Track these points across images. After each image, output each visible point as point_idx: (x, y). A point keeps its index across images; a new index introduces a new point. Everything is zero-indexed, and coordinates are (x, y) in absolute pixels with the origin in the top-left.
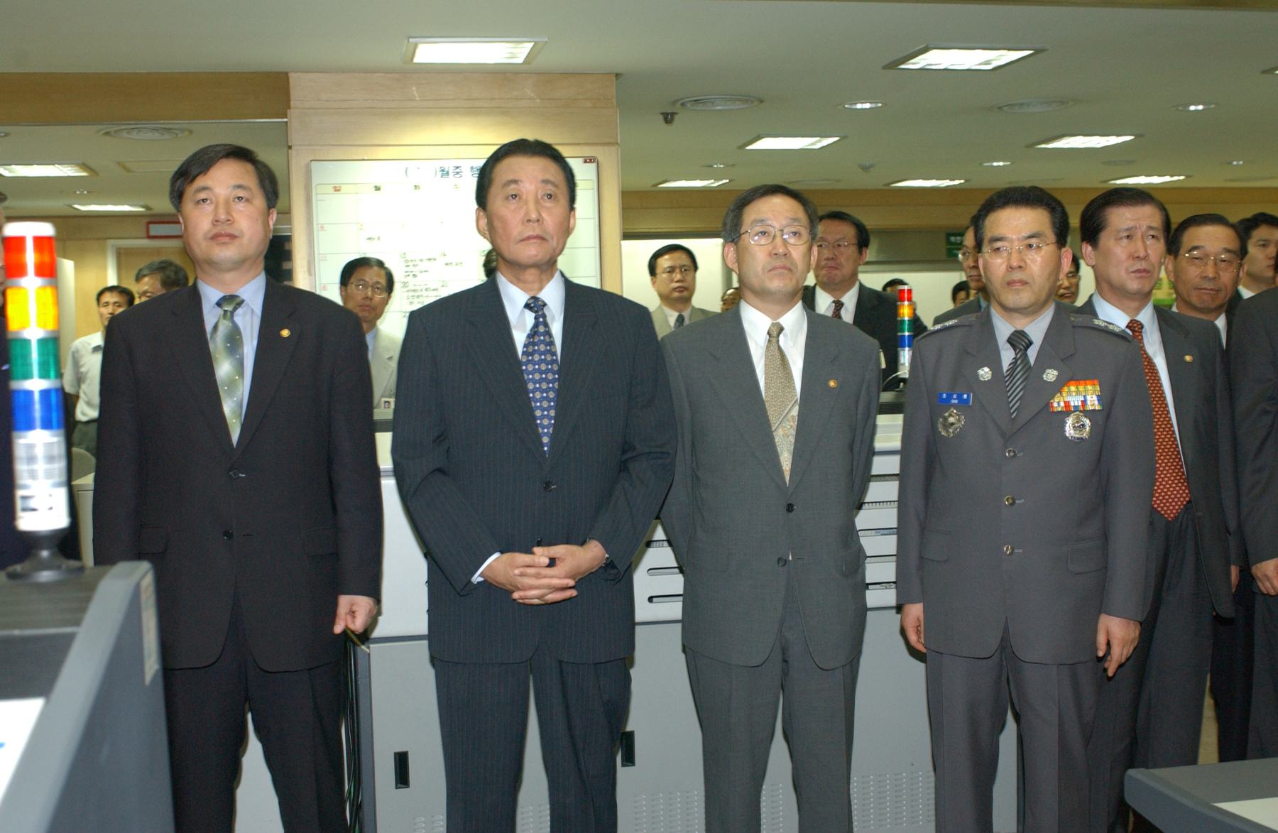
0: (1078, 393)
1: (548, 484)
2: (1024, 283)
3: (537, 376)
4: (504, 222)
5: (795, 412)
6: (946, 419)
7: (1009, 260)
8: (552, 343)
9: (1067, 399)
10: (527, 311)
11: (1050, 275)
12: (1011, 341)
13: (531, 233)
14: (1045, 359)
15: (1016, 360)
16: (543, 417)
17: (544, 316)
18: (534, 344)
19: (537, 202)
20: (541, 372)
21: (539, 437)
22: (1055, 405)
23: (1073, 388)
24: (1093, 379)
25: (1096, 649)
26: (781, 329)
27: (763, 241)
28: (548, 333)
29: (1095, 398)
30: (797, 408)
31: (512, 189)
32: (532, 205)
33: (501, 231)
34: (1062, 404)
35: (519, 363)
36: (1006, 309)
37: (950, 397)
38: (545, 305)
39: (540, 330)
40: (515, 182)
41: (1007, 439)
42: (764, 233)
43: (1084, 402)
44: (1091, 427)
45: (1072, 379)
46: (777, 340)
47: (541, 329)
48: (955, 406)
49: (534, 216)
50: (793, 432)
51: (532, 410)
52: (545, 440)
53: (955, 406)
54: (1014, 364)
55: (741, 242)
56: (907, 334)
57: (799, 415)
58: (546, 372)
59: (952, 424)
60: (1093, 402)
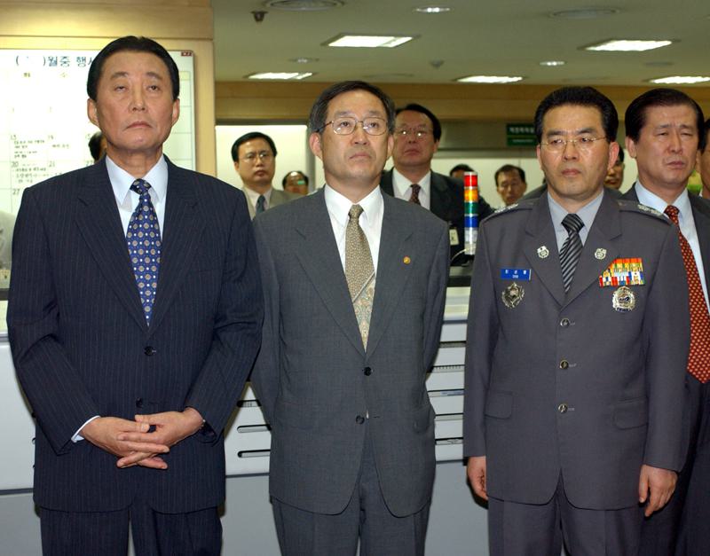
0: (624, 269)
1: (148, 349)
2: (577, 172)
3: (141, 252)
4: (112, 109)
5: (373, 285)
6: (508, 292)
7: (564, 152)
8: (156, 222)
9: (615, 275)
10: (133, 192)
11: (600, 166)
12: (564, 223)
13: (136, 120)
14: (597, 238)
15: (569, 240)
16: (145, 289)
17: (149, 197)
18: (138, 222)
19: (143, 92)
20: (145, 248)
21: (141, 307)
22: (604, 280)
23: (619, 265)
25: (638, 496)
26: (362, 210)
27: (345, 132)
28: (155, 215)
29: (638, 273)
30: (374, 282)
31: (120, 81)
32: (138, 95)
33: (109, 119)
34: (610, 279)
35: (125, 240)
36: (562, 195)
37: (511, 272)
38: (150, 186)
39: (144, 210)
40: (123, 74)
41: (562, 310)
42: (346, 124)
43: (629, 278)
45: (618, 258)
46: (356, 220)
47: (146, 209)
49: (139, 105)
50: (371, 303)
51: (135, 284)
52: (147, 309)
54: (568, 243)
55: (325, 132)
56: (471, 215)
57: (375, 288)
58: (149, 248)
59: (514, 296)
60: (637, 278)
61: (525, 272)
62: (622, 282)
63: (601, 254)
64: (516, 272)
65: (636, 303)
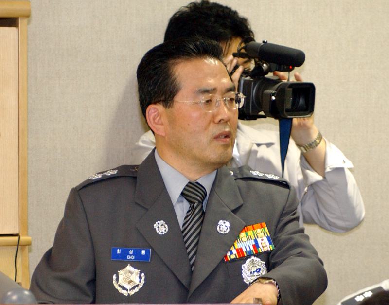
24: (261, 223)
43: (256, 246)
48: (134, 264)
61: (143, 252)
62: (250, 251)
64: (131, 252)
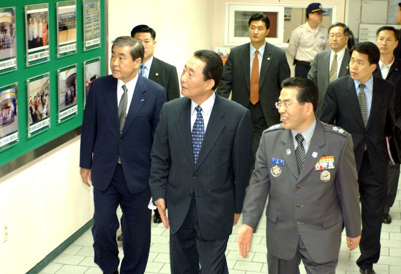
9: (321, 165)
22: (317, 167)
29: (332, 164)
34: (319, 167)
37: (276, 161)
43: (328, 166)
44: (331, 175)
53: (277, 164)
60: (332, 166)
61: (282, 162)
62: (325, 169)
63: (315, 155)
65: (331, 177)
